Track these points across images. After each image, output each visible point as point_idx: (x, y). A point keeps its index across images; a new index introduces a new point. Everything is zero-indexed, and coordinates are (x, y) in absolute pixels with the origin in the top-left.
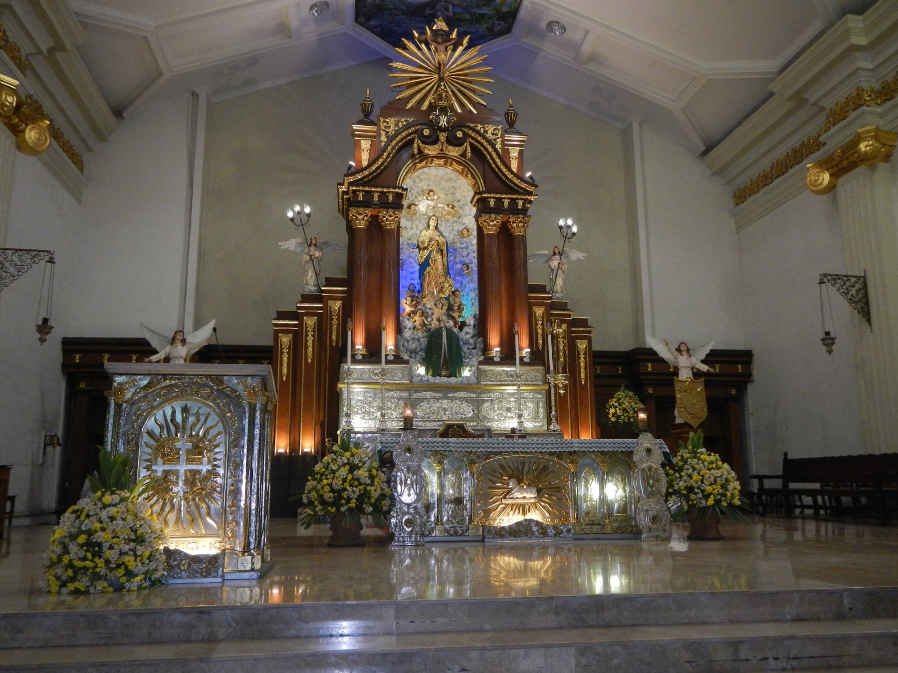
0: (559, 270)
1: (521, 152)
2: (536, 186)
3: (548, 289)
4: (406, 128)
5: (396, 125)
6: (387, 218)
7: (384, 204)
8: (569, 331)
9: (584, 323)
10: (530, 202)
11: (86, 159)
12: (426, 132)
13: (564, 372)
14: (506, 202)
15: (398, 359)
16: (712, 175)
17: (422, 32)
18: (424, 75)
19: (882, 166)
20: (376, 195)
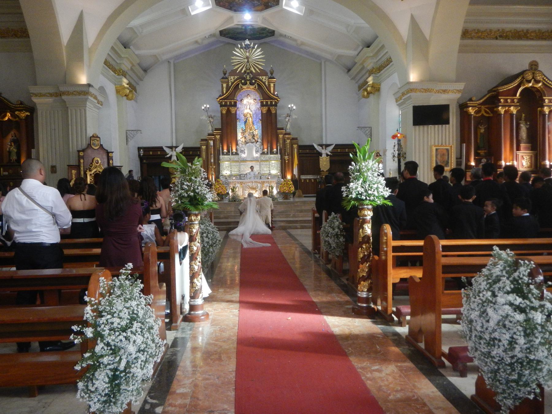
0: (289, 123)
1: (274, 85)
2: (278, 97)
3: (284, 129)
4: (236, 80)
5: (234, 79)
6: (233, 110)
7: (231, 105)
8: (291, 142)
9: (296, 139)
10: (278, 101)
11: (138, 88)
12: (243, 81)
13: (288, 155)
14: (269, 103)
15: (237, 154)
16: (351, 79)
17: (241, 45)
18: (243, 61)
19: (377, 93)
20: (228, 103)
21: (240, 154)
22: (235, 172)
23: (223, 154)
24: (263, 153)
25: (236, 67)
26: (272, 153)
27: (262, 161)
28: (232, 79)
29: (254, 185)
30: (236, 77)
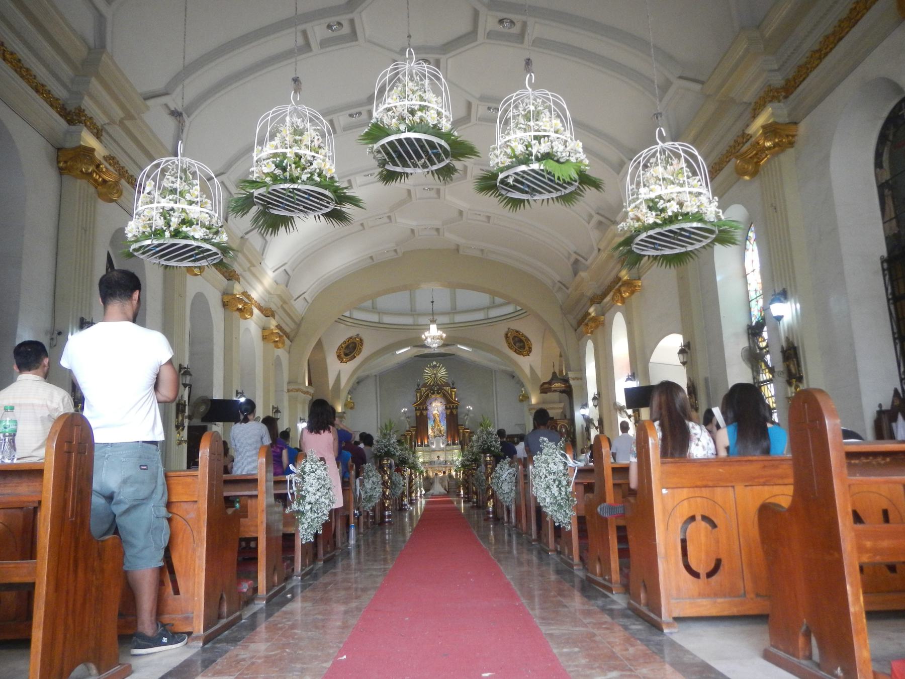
4: (428, 390)
6: (425, 412)
7: (423, 409)
8: (469, 435)
15: (428, 446)
17: (430, 365)
21: (430, 445)
22: (427, 459)
23: (418, 446)
24: (448, 445)
25: (427, 381)
26: (454, 444)
27: (447, 450)
28: (423, 390)
29: (440, 469)
30: (427, 389)
